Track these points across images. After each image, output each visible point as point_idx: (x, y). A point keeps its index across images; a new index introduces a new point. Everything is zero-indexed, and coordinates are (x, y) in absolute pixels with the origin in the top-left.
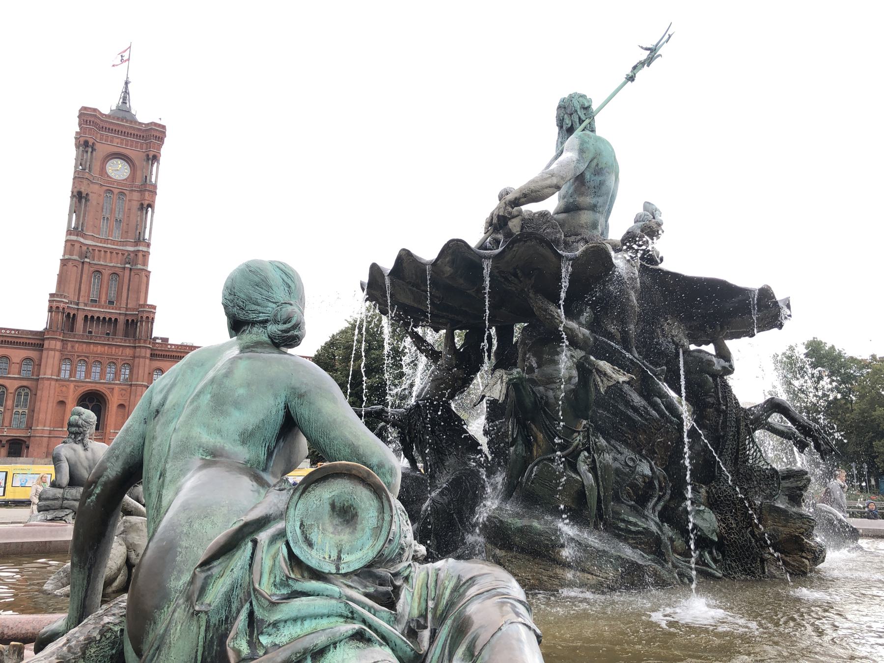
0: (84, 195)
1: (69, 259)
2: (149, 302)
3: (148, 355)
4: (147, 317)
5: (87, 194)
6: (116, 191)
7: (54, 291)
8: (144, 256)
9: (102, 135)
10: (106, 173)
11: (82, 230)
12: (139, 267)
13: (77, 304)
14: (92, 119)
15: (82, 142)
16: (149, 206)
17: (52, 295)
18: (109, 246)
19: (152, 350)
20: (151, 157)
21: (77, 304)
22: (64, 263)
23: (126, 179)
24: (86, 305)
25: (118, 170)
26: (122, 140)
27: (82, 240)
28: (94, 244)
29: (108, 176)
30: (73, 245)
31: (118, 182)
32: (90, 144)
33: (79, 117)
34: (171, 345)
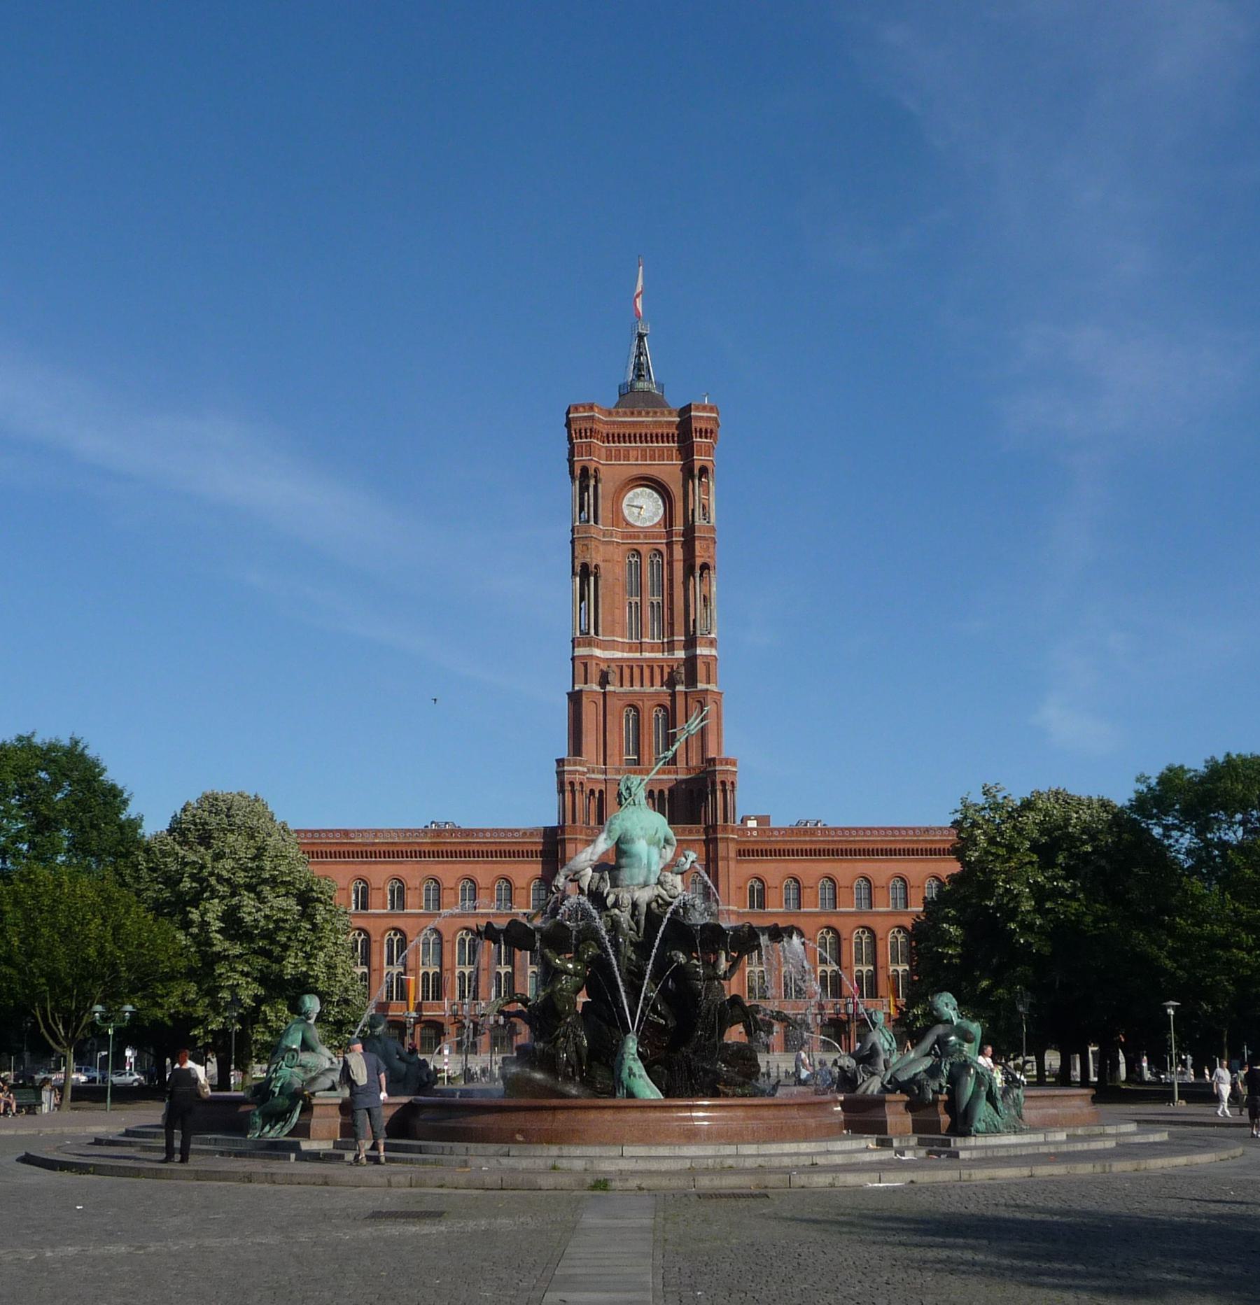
0: (592, 568)
1: (581, 691)
2: (724, 755)
3: (732, 854)
4: (723, 783)
5: (596, 567)
6: (644, 550)
7: (564, 754)
8: (708, 665)
9: (609, 450)
10: (625, 520)
11: (596, 633)
12: (701, 686)
13: (605, 773)
14: (588, 426)
15: (578, 472)
16: (705, 567)
17: (560, 762)
18: (647, 655)
19: (738, 842)
20: (696, 472)
21: (605, 773)
22: (575, 698)
23: (658, 523)
24: (618, 771)
25: (644, 508)
26: (644, 450)
27: (597, 652)
28: (618, 655)
29: (628, 524)
30: (586, 665)
31: (647, 533)
32: (591, 472)
33: (568, 424)
34: (779, 830)
